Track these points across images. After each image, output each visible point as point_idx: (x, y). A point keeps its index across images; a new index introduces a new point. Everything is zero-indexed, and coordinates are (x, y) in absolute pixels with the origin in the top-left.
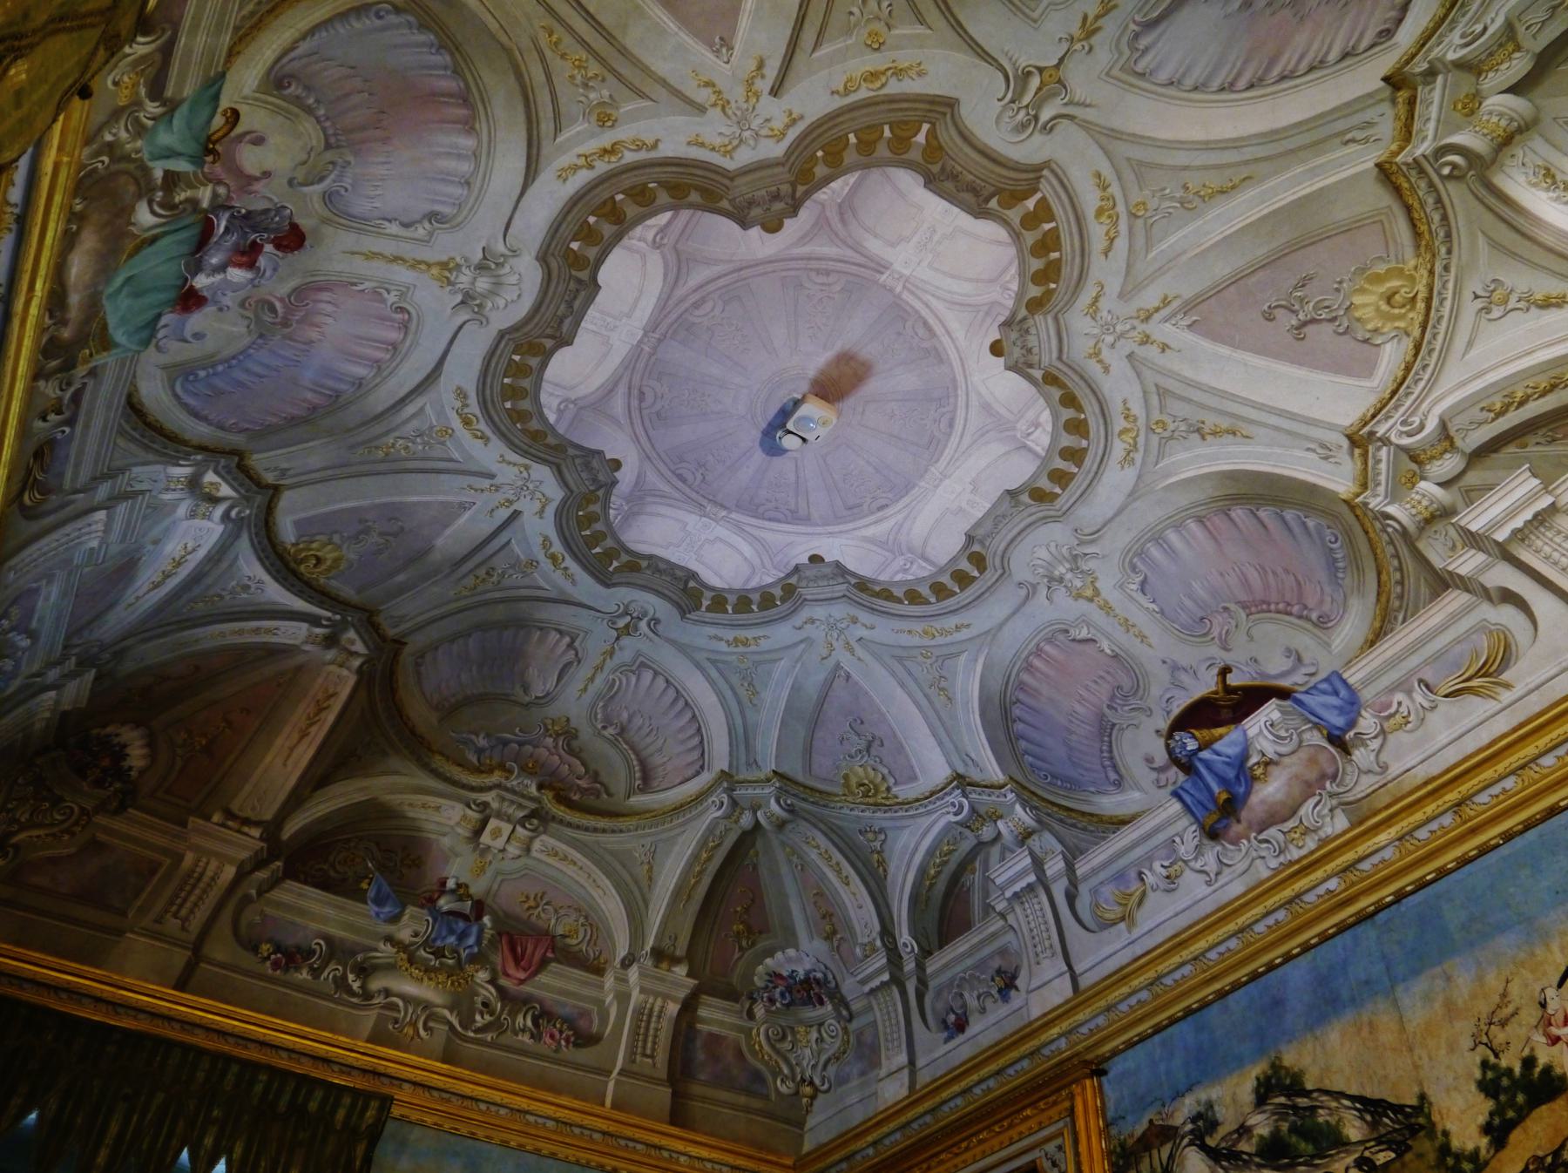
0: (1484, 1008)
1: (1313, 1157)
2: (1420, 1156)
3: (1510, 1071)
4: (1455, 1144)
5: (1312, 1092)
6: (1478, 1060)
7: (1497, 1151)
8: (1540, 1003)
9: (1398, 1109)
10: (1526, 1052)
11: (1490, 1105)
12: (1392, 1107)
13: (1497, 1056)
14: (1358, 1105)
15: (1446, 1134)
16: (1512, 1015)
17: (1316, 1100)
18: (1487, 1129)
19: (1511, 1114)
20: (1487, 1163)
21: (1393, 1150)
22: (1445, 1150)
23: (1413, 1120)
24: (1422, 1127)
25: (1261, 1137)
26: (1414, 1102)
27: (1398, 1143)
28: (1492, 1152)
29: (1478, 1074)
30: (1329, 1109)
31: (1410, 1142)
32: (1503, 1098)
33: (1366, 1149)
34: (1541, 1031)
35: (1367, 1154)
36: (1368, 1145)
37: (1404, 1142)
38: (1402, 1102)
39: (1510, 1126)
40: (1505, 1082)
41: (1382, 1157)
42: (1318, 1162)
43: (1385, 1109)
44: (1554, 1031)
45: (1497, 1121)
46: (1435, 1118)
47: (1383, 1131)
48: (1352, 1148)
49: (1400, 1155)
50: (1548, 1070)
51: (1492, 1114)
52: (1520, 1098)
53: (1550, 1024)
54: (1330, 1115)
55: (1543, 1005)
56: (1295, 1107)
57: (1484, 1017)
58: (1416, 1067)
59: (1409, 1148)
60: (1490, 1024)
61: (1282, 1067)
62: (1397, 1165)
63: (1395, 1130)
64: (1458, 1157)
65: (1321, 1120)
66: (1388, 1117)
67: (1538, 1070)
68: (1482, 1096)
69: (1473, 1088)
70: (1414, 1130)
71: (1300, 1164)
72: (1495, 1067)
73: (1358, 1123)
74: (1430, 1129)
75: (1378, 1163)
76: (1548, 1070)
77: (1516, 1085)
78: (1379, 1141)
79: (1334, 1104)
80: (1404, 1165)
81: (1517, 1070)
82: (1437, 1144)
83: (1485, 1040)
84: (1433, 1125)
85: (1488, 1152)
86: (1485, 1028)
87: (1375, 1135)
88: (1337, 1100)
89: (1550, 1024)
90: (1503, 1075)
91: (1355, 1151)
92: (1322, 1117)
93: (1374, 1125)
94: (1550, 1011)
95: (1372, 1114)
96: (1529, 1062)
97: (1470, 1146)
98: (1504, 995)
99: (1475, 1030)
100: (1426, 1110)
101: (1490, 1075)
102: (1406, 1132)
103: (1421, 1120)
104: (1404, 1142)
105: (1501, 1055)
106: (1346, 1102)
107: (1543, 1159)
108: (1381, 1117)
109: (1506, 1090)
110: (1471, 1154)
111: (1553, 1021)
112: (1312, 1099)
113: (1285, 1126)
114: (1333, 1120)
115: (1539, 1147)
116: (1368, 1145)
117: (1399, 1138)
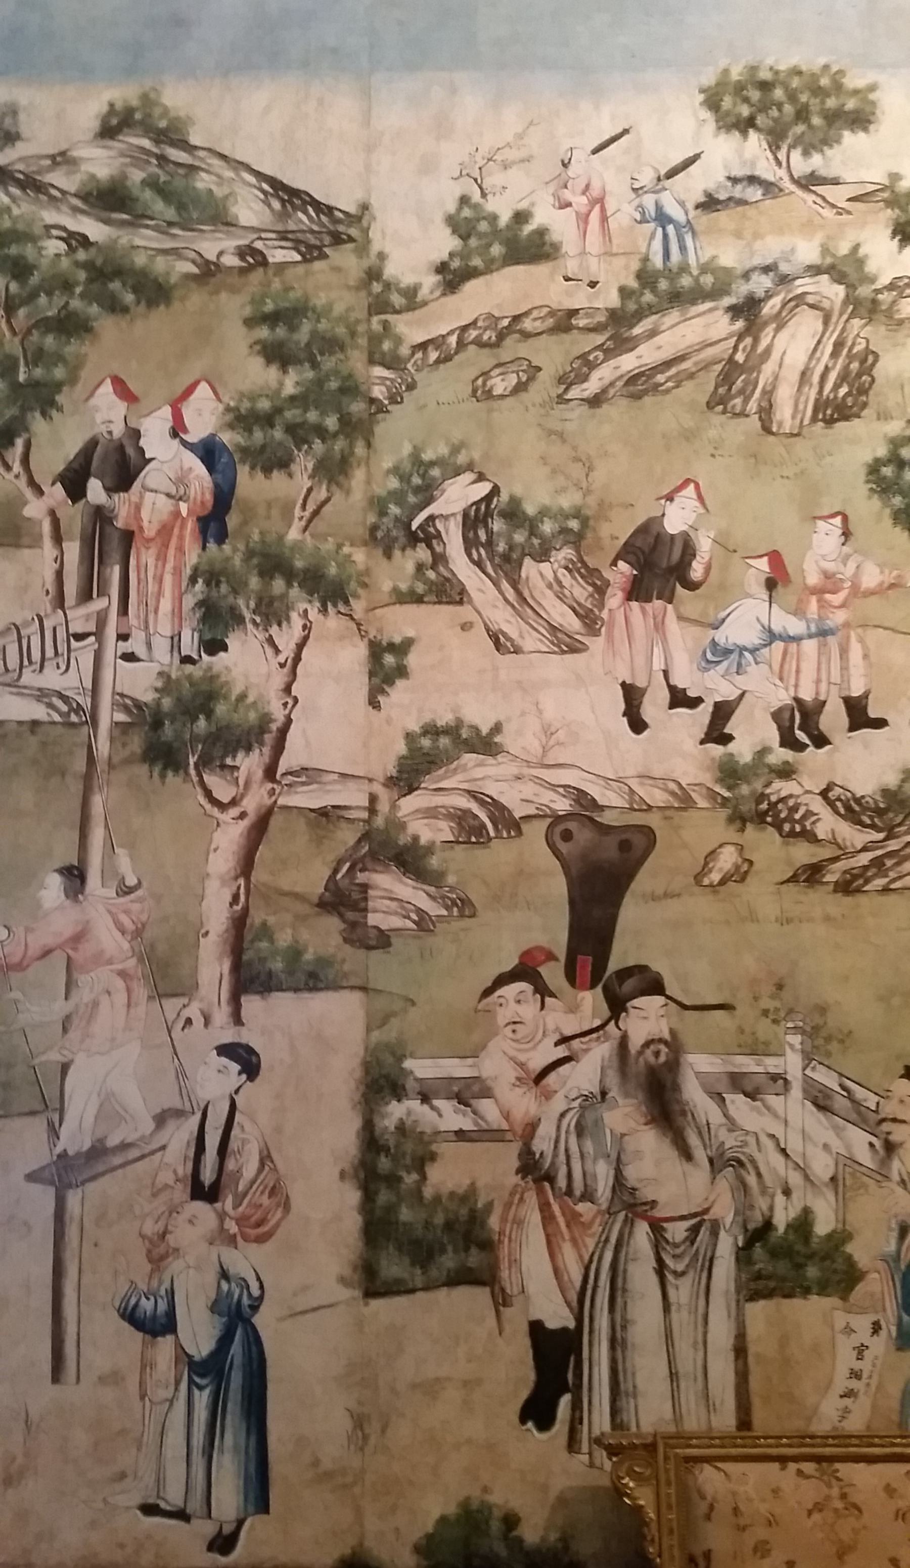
0: (488, 143)
1: (170, 224)
2: (337, 269)
3: (493, 218)
4: (390, 271)
5: (196, 148)
6: (458, 194)
7: (444, 294)
8: (563, 161)
9: (329, 210)
10: (523, 205)
11: (454, 243)
12: (317, 205)
13: (484, 195)
14: (265, 186)
15: (382, 256)
16: (522, 161)
17: (202, 159)
18: (442, 268)
19: (477, 262)
20: (425, 304)
21: (299, 252)
22: (373, 274)
23: (341, 228)
24: (351, 239)
25: (93, 177)
26: (352, 209)
27: (310, 247)
28: (438, 293)
29: (451, 207)
30: (219, 176)
31: (327, 250)
32: (473, 242)
33: (260, 238)
34: (551, 188)
35: (259, 245)
36: (263, 235)
37: (319, 248)
38: (332, 203)
39: (470, 274)
40: (483, 226)
41: (278, 255)
42: (176, 231)
43: (305, 203)
44: (567, 195)
45: (456, 264)
46: (374, 234)
47: (291, 226)
48: (240, 232)
49: (305, 260)
50: (541, 233)
51: (451, 255)
52: (497, 250)
53: (566, 187)
54: (219, 185)
55: (565, 165)
56: (162, 159)
57: (484, 151)
58: (368, 168)
59: (323, 256)
60: (489, 160)
61: (156, 103)
62: (300, 269)
63: (312, 232)
64: (388, 286)
65: (200, 185)
66: (305, 212)
67: (528, 229)
68: (448, 231)
69: (439, 219)
70: (338, 239)
71: (147, 227)
72: (476, 207)
73: (259, 206)
74: (363, 248)
75: (271, 260)
76: (541, 233)
77: (495, 233)
78: (283, 236)
79: (229, 174)
80: (307, 273)
81: (505, 218)
82: (366, 263)
83: (476, 174)
84: (368, 241)
85: (432, 292)
86: (481, 163)
87: (280, 227)
88: (235, 169)
89: (566, 187)
90: (484, 218)
91: (241, 237)
92: (203, 181)
93: (283, 216)
94: (571, 172)
95: (283, 201)
96: (521, 217)
97: (408, 280)
98: (520, 136)
99: (466, 159)
100: (365, 223)
101: (467, 213)
102: (327, 240)
103: (353, 232)
104: (319, 248)
105: (489, 197)
106: (252, 179)
107: (498, 319)
108: (295, 208)
109: (481, 236)
110: (408, 288)
111: (569, 185)
112: (194, 156)
113: (137, 176)
114: (219, 192)
115: (499, 306)
116: (263, 235)
117: (313, 241)
